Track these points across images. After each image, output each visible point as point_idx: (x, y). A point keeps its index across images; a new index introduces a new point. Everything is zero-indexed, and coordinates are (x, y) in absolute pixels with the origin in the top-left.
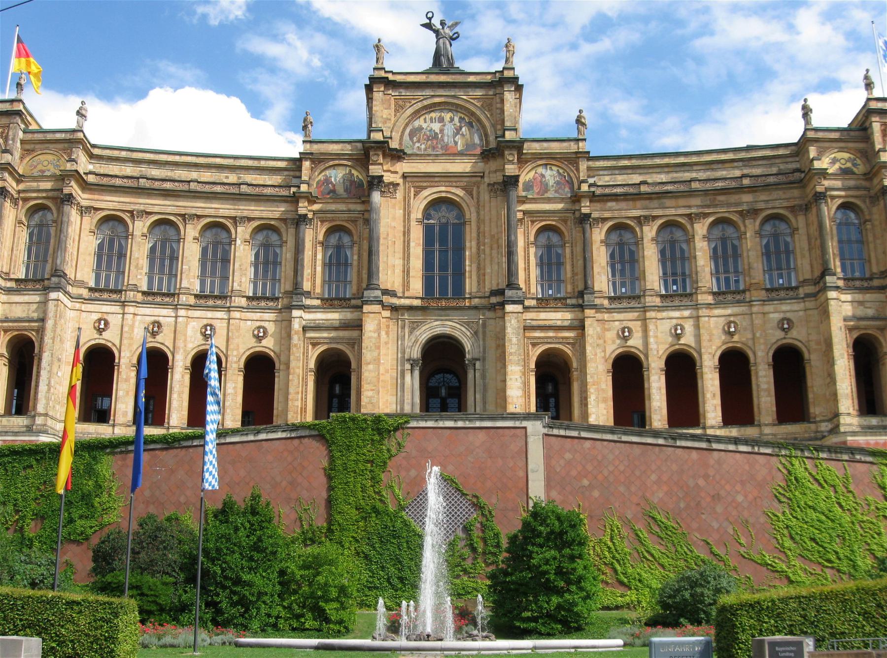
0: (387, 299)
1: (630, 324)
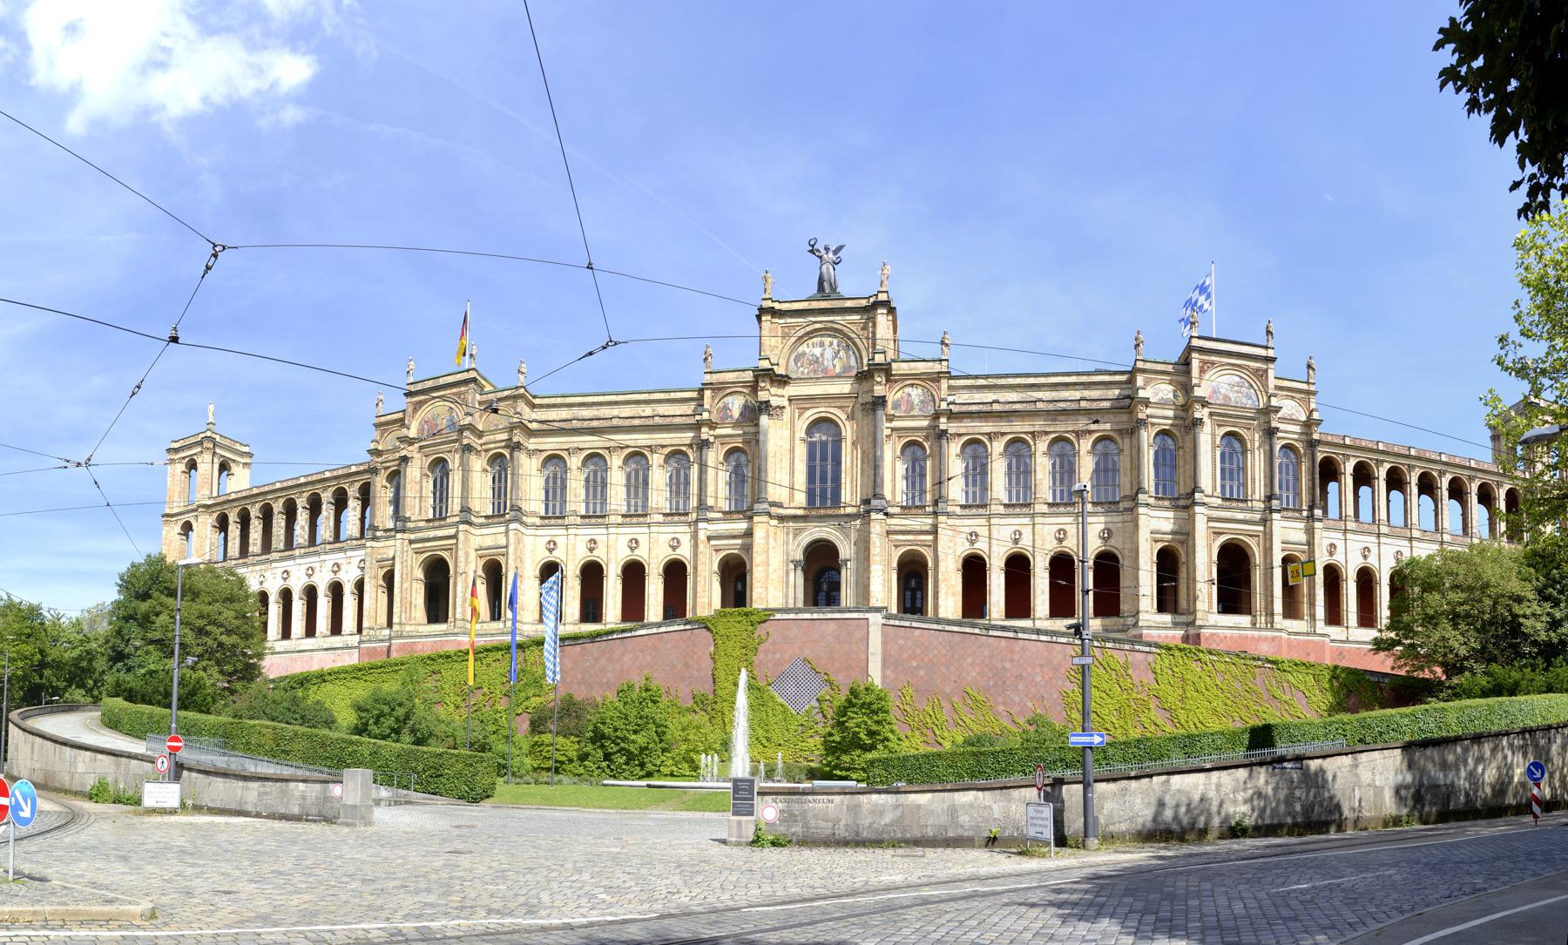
0: (774, 510)
1: (978, 530)
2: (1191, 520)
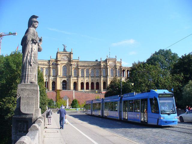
0: (59, 76)
2: (107, 79)
